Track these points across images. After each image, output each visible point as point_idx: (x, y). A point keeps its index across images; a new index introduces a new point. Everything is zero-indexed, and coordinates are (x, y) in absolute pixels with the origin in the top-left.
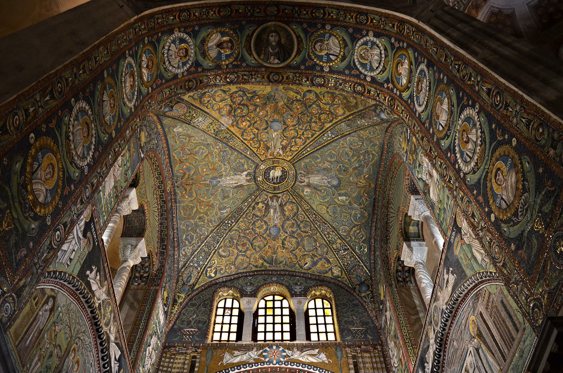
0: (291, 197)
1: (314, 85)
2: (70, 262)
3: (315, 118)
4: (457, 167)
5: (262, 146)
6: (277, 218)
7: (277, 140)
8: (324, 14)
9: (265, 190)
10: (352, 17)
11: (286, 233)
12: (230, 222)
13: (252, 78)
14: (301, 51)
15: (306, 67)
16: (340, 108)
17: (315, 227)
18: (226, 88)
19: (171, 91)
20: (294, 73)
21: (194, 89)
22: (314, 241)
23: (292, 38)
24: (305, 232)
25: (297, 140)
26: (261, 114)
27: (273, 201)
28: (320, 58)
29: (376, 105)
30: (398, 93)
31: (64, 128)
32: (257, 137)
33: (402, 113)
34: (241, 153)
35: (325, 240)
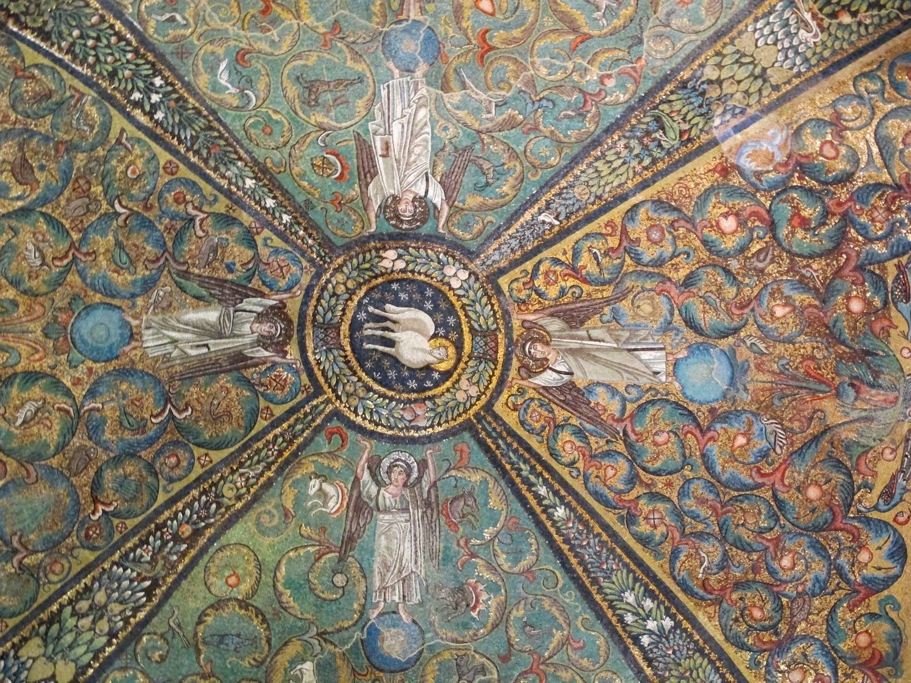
0: (279, 411)
3: (748, 564)
5: (586, 287)
6: (174, 341)
7: (620, 368)
9: (318, 276)
11: (92, 393)
12: (155, 98)
17: (125, 539)
22: (46, 540)
24: (96, 485)
25: (623, 466)
26: (780, 312)
27: (260, 317)
32: (639, 274)
34: (548, 185)
35: (62, 592)
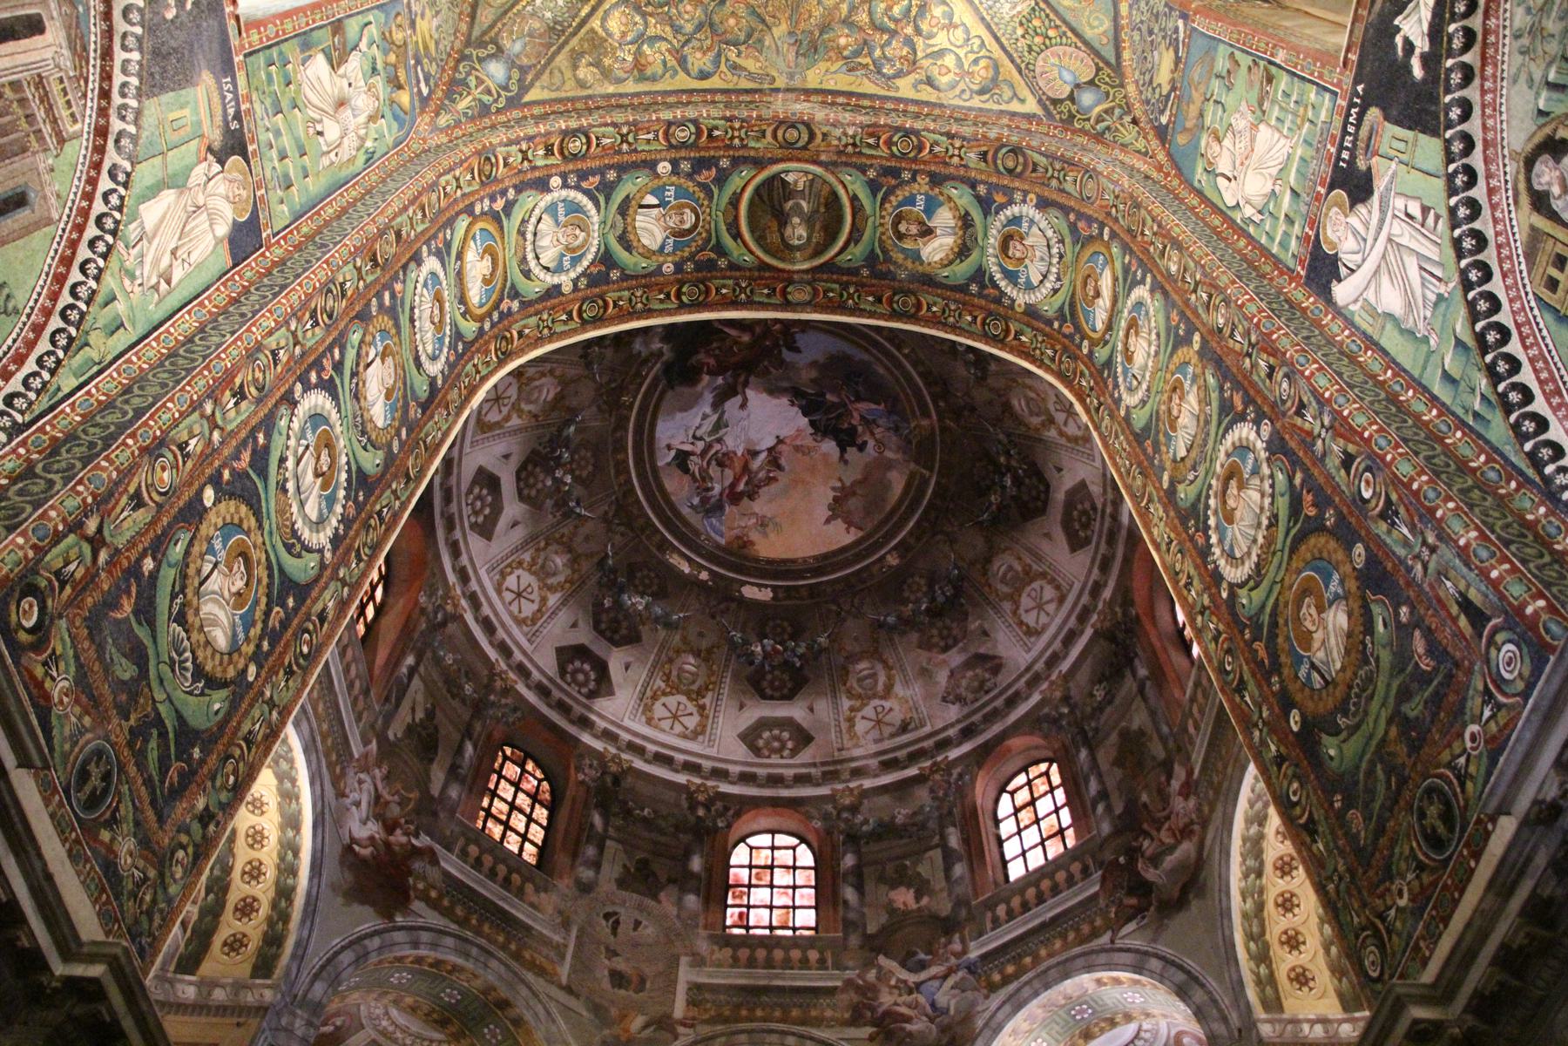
1: (695, 122)
4: (313, 377)
8: (679, 294)
10: (615, 305)
13: (854, 137)
14: (730, 203)
15: (717, 166)
16: (617, 35)
18: (927, 94)
20: (744, 147)
21: (1004, 146)
23: (752, 231)
28: (681, 193)
29: (524, 88)
30: (478, 210)
31: (1257, 595)
33: (457, 180)
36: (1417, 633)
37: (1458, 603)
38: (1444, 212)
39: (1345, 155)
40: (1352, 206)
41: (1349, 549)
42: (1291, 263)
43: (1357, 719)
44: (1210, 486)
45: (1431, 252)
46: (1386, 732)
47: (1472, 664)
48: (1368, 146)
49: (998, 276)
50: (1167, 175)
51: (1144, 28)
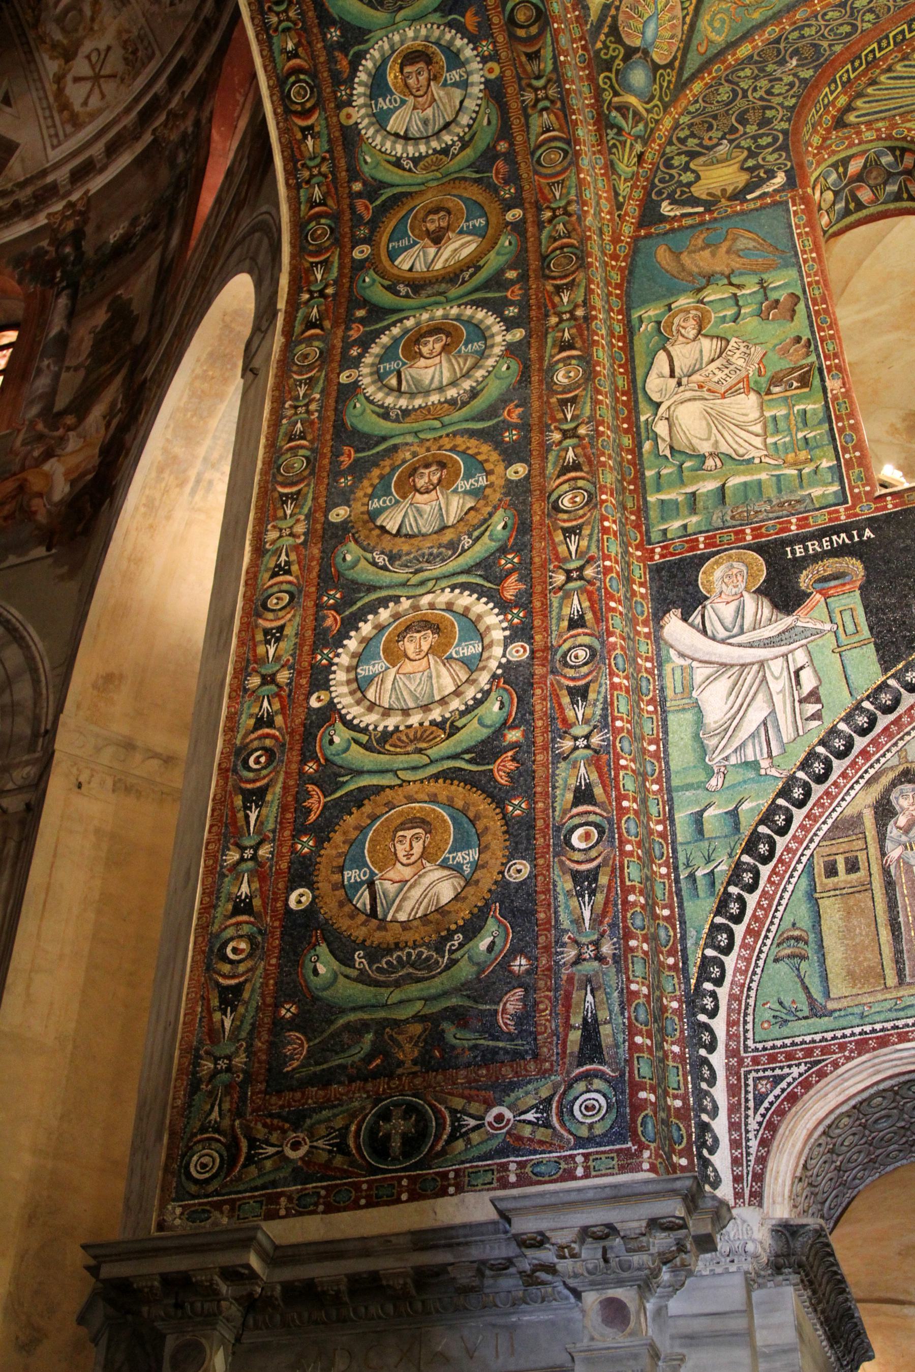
2: (818, 700)
19: (541, 105)
36: (519, 992)
37: (585, 1019)
38: (828, 725)
39: (799, 551)
40: (758, 591)
41: (514, 853)
42: (655, 536)
43: (382, 978)
44: (396, 599)
45: (787, 733)
46: (406, 1021)
47: (551, 1071)
48: (825, 579)
49: (369, 64)
50: (615, 257)
51: (740, 104)
